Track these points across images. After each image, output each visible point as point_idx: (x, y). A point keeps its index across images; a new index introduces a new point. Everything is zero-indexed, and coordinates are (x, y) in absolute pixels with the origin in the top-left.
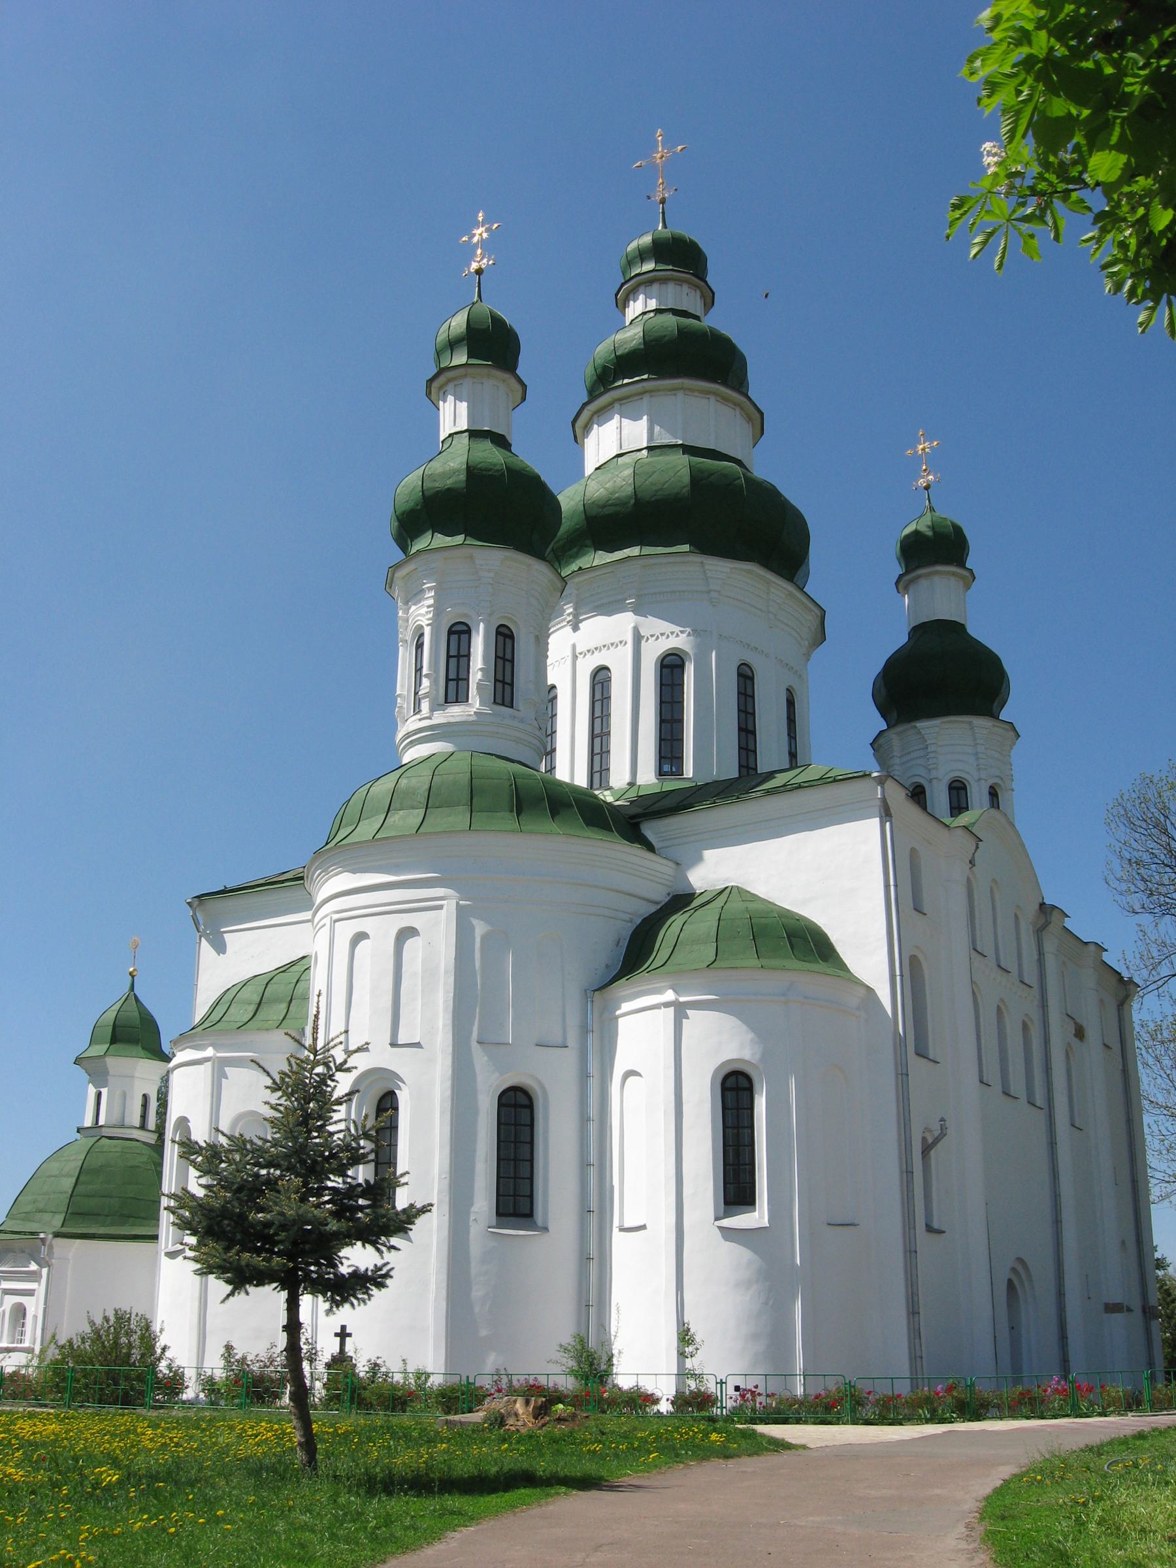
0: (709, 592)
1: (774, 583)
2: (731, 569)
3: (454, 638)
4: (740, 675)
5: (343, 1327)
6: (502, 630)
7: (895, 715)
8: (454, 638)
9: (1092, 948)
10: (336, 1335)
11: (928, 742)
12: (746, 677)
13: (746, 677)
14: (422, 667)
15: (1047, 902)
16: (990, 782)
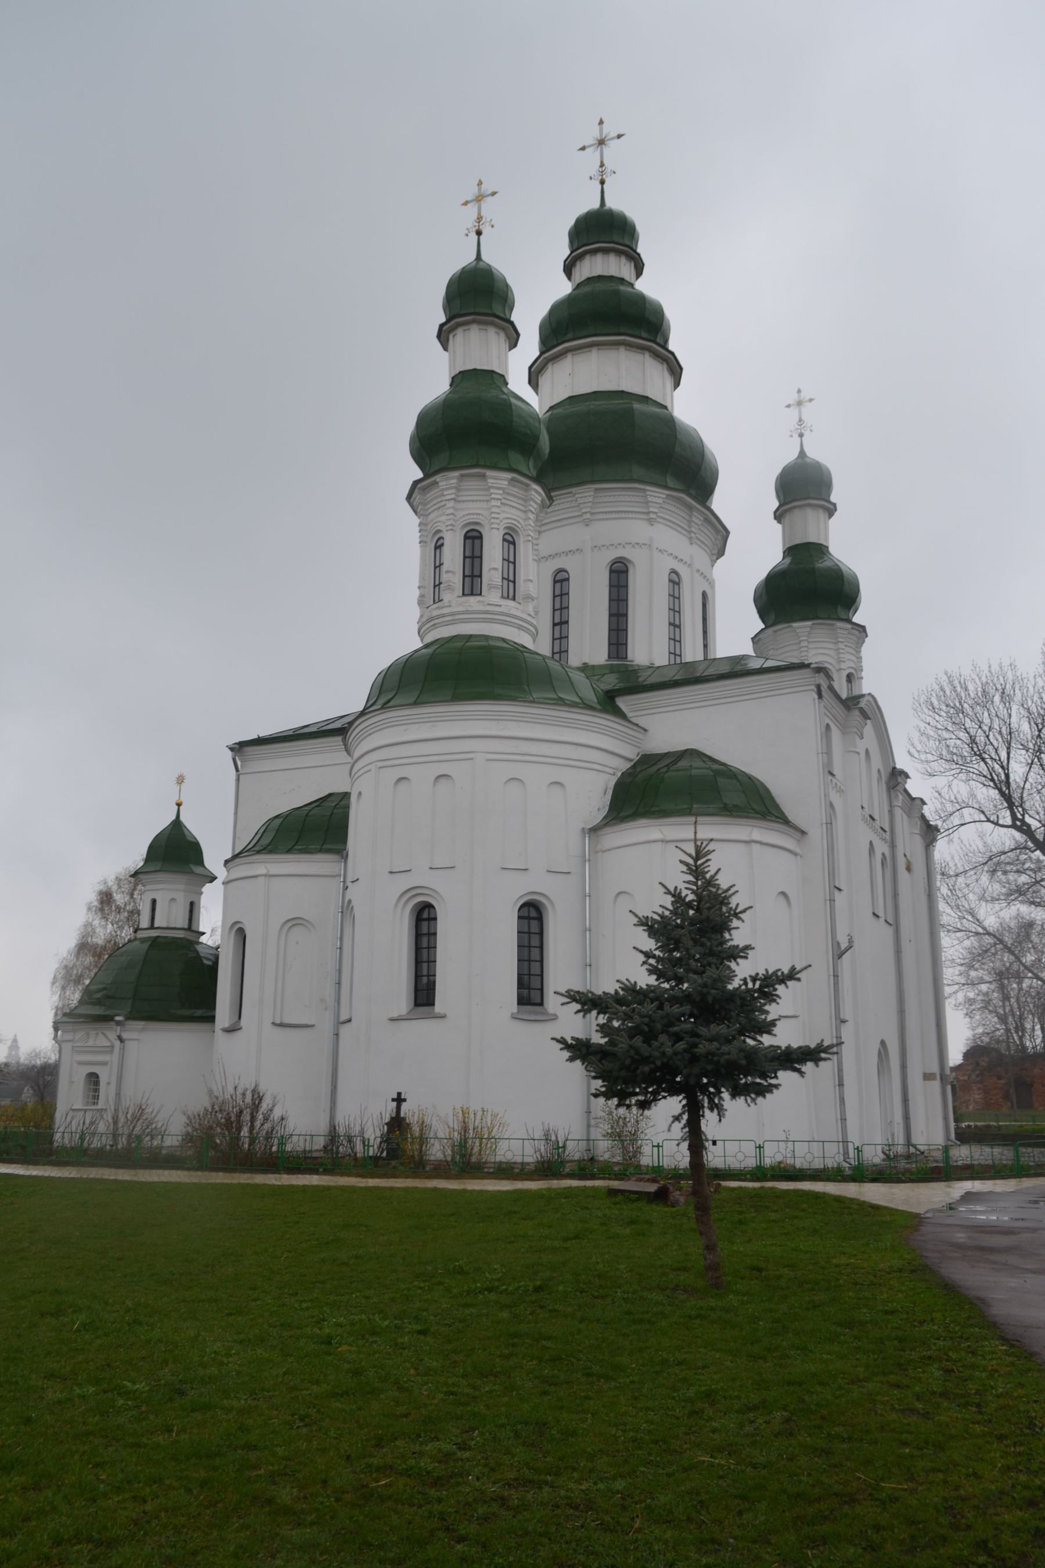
0: (649, 513)
1: (696, 508)
2: (668, 495)
3: (469, 542)
4: (670, 581)
5: (399, 1094)
6: (508, 537)
7: (772, 616)
8: (469, 542)
9: (919, 802)
10: (393, 1100)
11: (802, 639)
12: (675, 581)
13: (675, 581)
14: (441, 564)
15: (898, 766)
16: (848, 671)
